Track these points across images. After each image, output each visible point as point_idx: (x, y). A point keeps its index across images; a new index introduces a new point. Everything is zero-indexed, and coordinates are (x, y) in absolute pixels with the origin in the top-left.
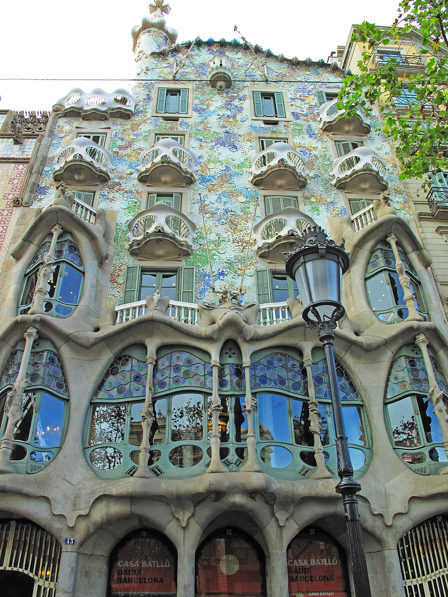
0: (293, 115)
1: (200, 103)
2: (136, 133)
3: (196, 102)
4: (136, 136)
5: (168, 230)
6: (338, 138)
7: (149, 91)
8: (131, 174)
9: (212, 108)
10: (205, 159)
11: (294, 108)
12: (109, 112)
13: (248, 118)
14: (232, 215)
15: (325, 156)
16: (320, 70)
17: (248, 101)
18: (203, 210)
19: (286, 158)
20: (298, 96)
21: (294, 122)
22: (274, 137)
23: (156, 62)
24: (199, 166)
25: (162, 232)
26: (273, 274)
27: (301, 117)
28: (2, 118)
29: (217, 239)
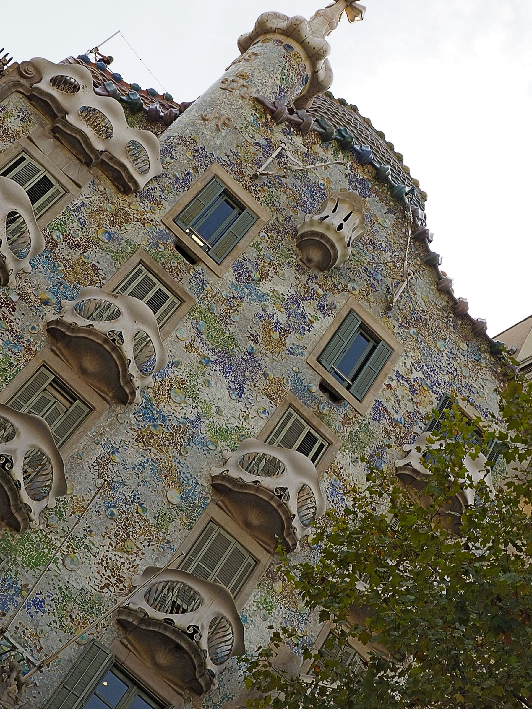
0: (375, 407)
2: (113, 230)
3: (252, 254)
4: (109, 238)
5: (17, 473)
7: (196, 170)
8: (46, 302)
9: (265, 287)
11: (388, 394)
12: (103, 157)
13: (303, 354)
14: (137, 513)
16: (485, 358)
17: (330, 319)
18: (101, 465)
19: (292, 492)
20: (411, 377)
21: (367, 421)
22: (315, 423)
24: (159, 380)
25: (5, 470)
26: (115, 665)
27: (384, 421)
29: (80, 535)
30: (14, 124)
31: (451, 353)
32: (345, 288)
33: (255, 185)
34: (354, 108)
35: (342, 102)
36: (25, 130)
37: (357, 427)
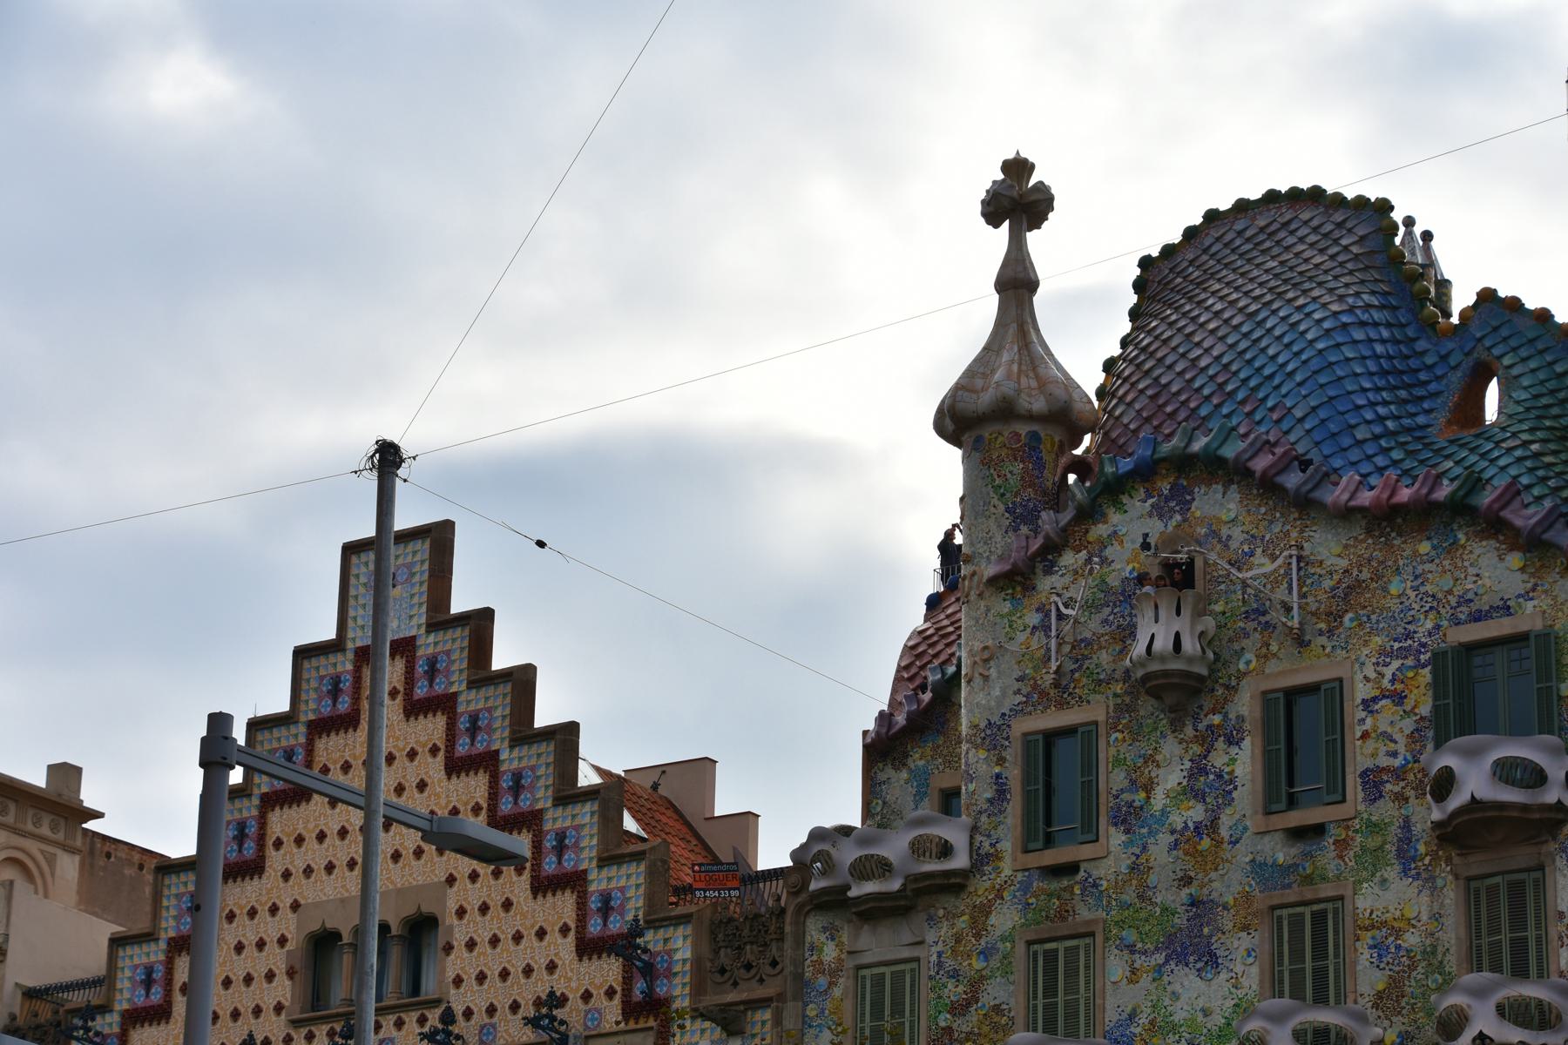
0: (1364, 783)
1: (1126, 783)
4: (986, 959)
6: (1477, 864)
7: (1001, 761)
9: (1159, 800)
10: (1143, 1020)
11: (1371, 744)
13: (1246, 829)
15: (1434, 953)
16: (1460, 527)
20: (1386, 683)
21: (1365, 816)
23: (1007, 607)
27: (1389, 787)
28: (685, 937)
30: (830, 953)
31: (1416, 577)
32: (1241, 675)
33: (1066, 687)
34: (1212, 216)
35: (1190, 233)
36: (839, 945)
37: (1359, 838)
